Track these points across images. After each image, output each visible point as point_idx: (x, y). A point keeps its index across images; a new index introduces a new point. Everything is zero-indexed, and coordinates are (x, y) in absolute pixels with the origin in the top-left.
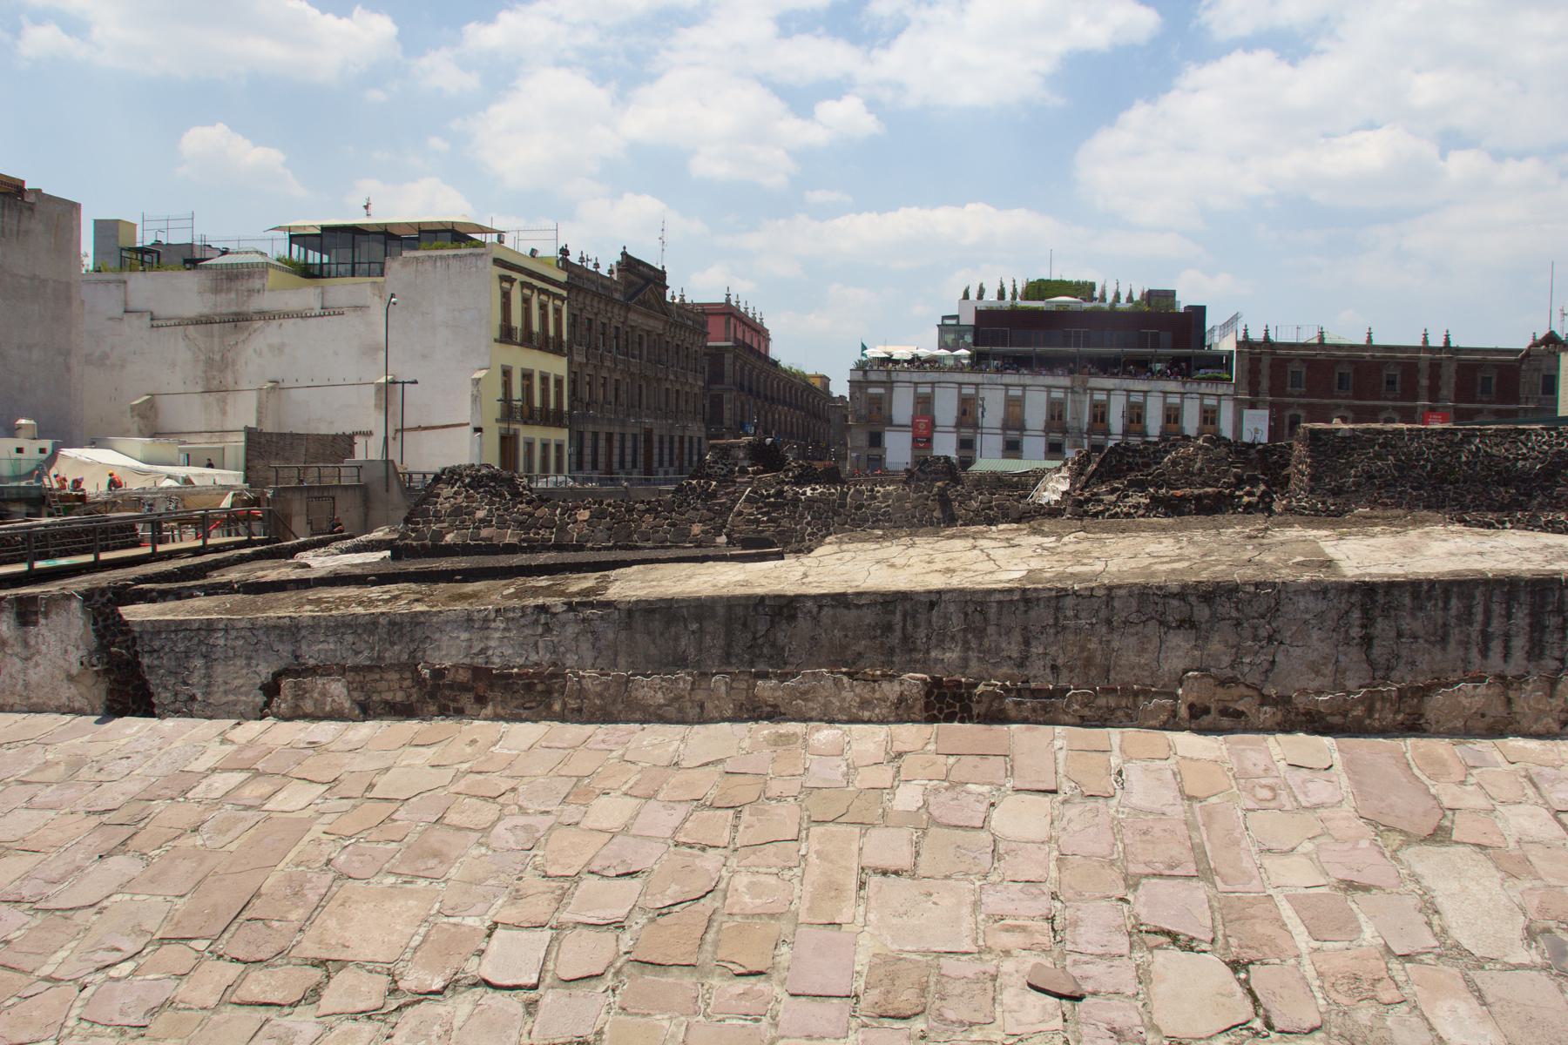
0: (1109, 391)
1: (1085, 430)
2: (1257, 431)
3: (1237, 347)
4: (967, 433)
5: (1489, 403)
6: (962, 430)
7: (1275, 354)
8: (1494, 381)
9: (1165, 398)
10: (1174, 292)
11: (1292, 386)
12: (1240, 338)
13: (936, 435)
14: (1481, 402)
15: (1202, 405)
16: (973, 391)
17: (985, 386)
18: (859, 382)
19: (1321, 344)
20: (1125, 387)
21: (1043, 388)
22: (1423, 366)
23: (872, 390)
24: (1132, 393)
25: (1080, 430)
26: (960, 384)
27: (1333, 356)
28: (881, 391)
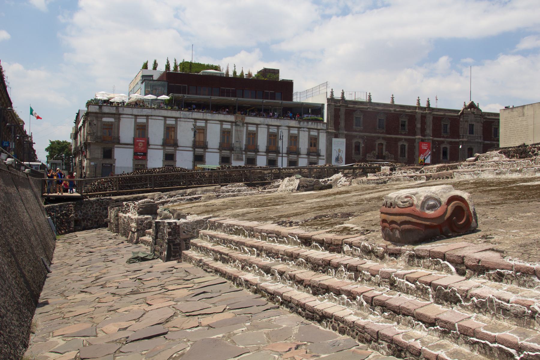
0: (257, 125)
1: (244, 149)
2: (339, 151)
3: (328, 102)
4: (170, 150)
5: (447, 138)
6: (167, 148)
7: (347, 107)
8: (448, 126)
9: (289, 131)
10: (279, 70)
11: (356, 125)
12: (329, 97)
13: (149, 151)
14: (443, 137)
15: (309, 135)
16: (174, 123)
17: (181, 120)
18: (96, 113)
19: (370, 102)
20: (266, 123)
21: (218, 122)
22: (418, 117)
23: (105, 119)
24: (270, 127)
25: (241, 149)
26: (165, 117)
27: (375, 109)
28: (112, 120)
